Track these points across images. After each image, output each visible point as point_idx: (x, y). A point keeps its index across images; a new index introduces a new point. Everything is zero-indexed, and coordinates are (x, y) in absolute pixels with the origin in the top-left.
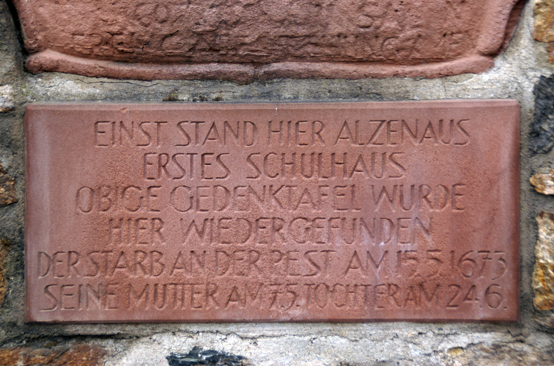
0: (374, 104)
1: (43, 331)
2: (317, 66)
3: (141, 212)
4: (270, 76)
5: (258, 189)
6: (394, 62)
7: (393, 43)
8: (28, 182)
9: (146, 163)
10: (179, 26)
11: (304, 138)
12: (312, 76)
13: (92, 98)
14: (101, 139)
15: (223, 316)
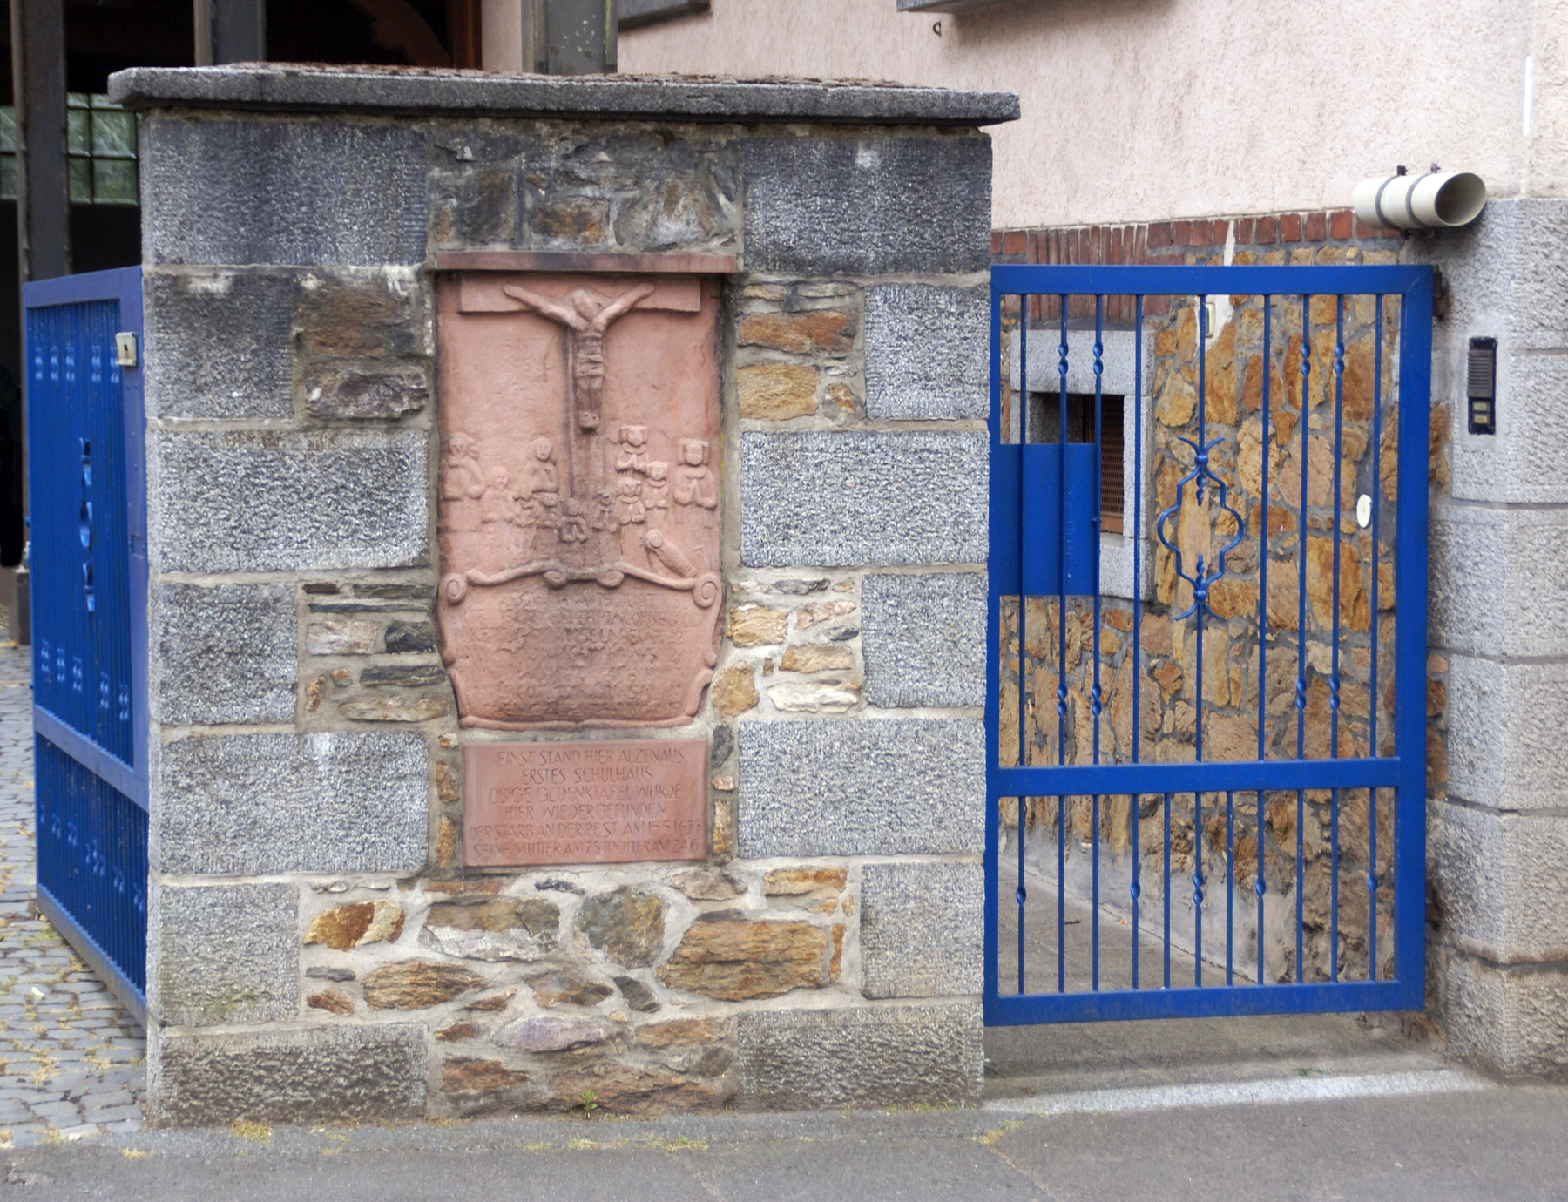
0: (638, 741)
1: (472, 872)
2: (608, 722)
3: (521, 803)
4: (584, 728)
5: (580, 789)
6: (645, 719)
7: (645, 708)
8: (464, 788)
9: (525, 775)
10: (539, 699)
11: (603, 760)
12: (605, 727)
13: (495, 741)
14: (502, 762)
15: (562, 861)
